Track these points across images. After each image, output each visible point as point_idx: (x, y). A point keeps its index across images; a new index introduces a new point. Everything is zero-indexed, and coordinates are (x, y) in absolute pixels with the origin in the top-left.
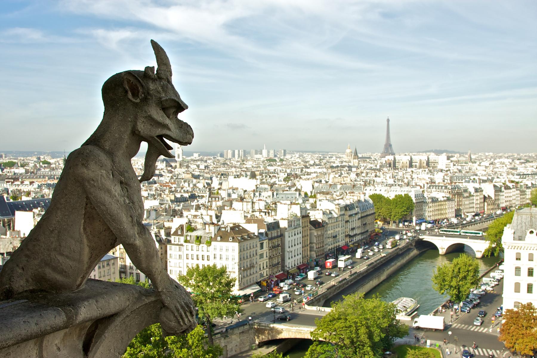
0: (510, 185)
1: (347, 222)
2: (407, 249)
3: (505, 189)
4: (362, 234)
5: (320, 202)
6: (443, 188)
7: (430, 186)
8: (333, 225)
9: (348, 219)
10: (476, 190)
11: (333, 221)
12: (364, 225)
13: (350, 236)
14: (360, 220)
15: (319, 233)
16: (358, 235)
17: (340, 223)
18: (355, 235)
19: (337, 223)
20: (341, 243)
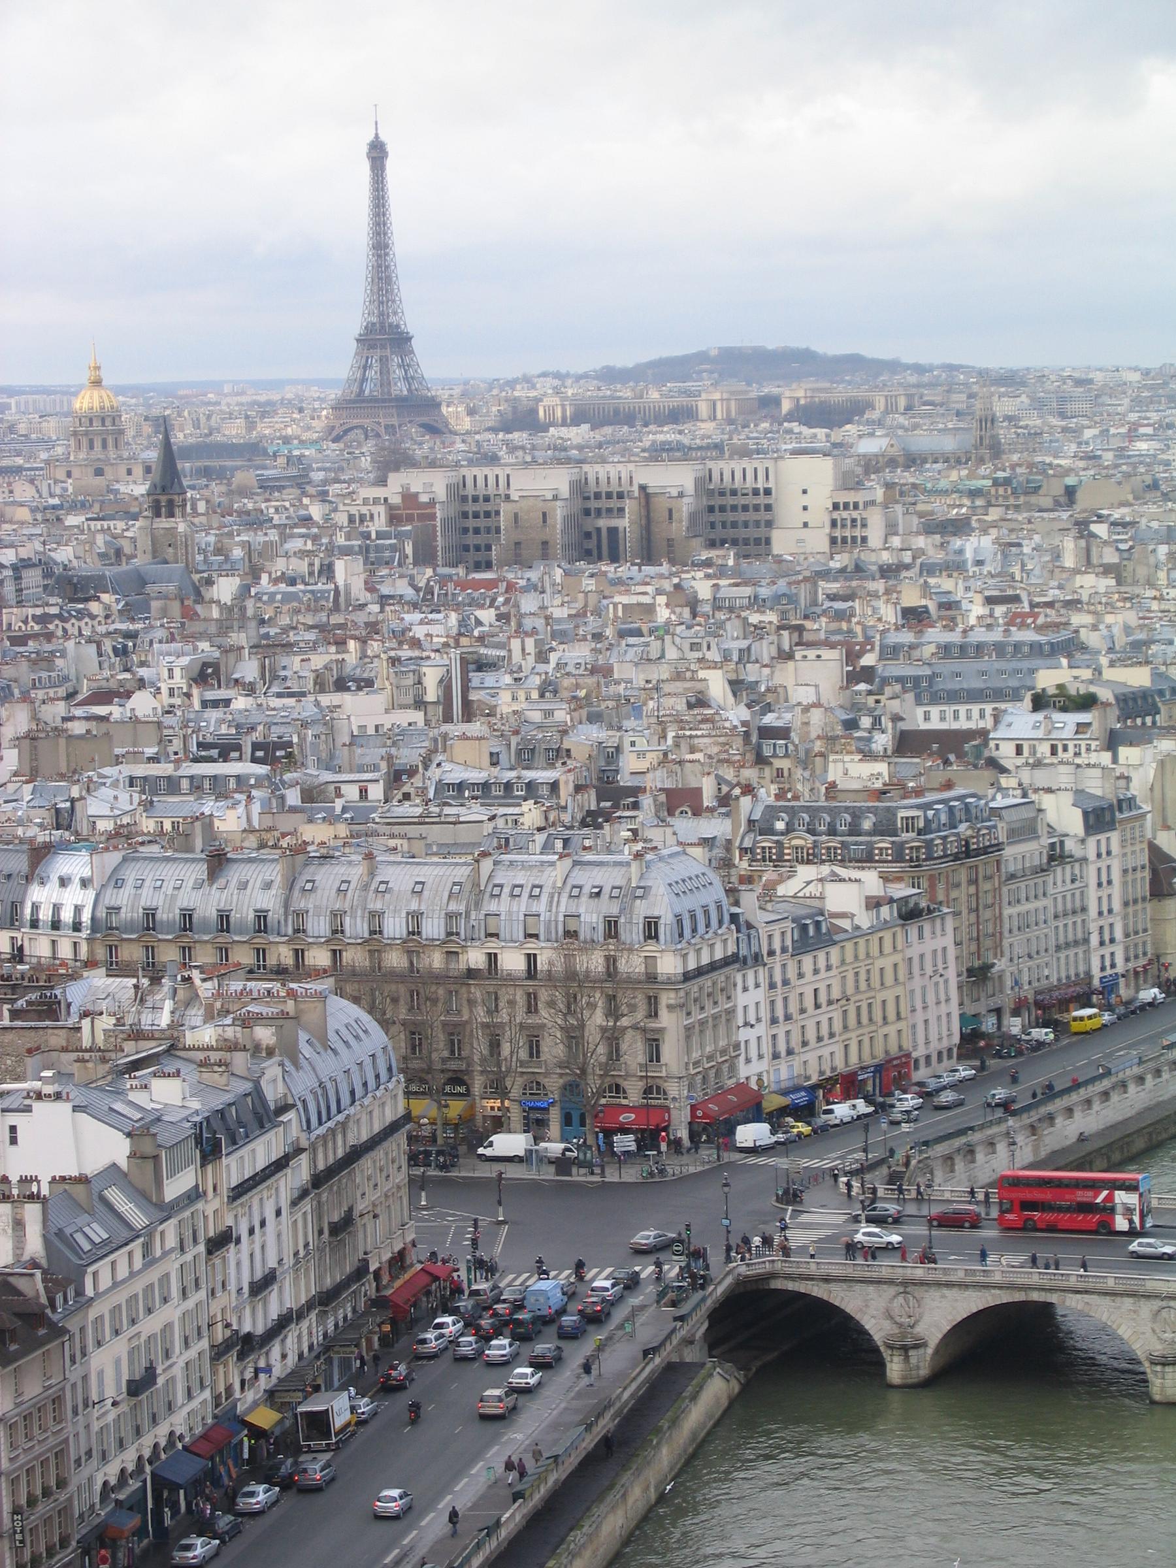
4: (325, 1300)
7: (771, 813)
8: (120, 1297)
10: (1099, 818)
11: (122, 1272)
14: (307, 1206)
15: (33, 1389)
17: (172, 1266)
19: (153, 1275)
20: (186, 1417)
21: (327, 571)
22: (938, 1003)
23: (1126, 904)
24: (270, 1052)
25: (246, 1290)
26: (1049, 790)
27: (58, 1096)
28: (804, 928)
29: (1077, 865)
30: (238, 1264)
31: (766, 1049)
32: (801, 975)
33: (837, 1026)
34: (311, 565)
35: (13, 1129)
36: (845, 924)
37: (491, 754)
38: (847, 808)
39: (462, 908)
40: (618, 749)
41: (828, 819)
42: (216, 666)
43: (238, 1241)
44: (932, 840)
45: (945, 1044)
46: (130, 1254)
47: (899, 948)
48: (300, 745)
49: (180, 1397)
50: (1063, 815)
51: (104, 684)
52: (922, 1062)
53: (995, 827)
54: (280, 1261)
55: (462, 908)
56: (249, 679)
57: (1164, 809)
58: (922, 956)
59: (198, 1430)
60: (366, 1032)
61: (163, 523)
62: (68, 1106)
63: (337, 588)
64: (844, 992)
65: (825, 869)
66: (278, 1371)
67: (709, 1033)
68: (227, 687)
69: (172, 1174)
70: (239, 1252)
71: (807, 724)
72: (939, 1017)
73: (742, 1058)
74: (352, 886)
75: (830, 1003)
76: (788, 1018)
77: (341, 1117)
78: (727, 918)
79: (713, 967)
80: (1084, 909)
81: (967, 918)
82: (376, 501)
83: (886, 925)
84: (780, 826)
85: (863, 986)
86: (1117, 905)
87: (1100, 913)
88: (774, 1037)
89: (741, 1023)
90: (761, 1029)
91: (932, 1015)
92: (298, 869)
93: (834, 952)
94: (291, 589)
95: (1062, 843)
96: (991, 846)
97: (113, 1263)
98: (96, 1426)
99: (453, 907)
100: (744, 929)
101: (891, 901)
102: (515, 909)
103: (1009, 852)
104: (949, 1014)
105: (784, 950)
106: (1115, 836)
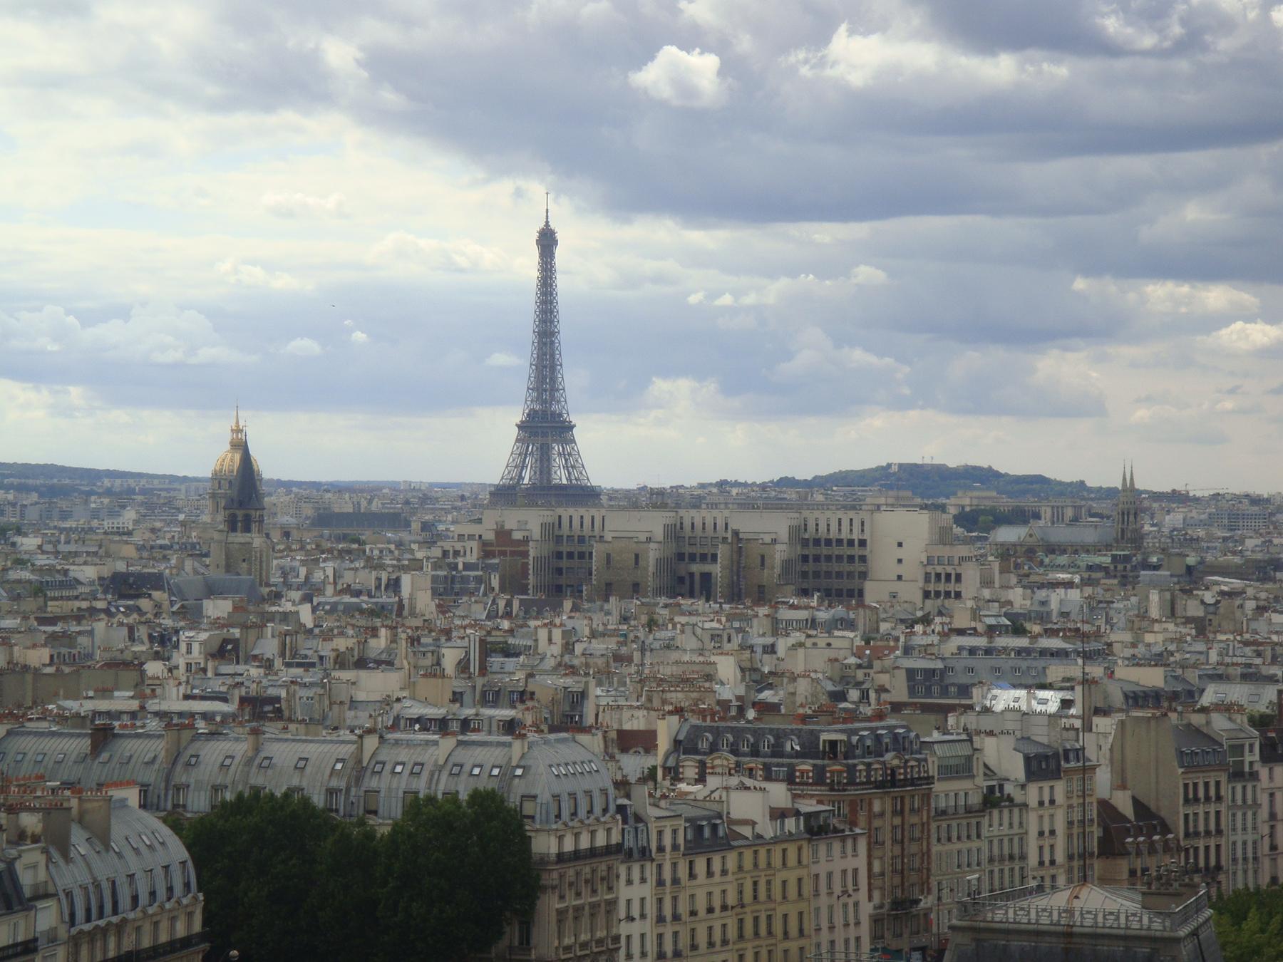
7: (696, 732)
10: (1043, 765)
21: (394, 585)
22: (847, 925)
23: (1070, 857)
24: (35, 839)
26: (991, 734)
29: (1016, 811)
32: (692, 876)
33: (732, 933)
34: (379, 579)
36: (746, 831)
37: (454, 693)
38: (771, 730)
39: (343, 785)
40: (583, 695)
41: (752, 740)
42: (236, 642)
44: (855, 765)
47: (805, 862)
48: (288, 700)
50: (1004, 759)
51: (118, 655)
53: (926, 760)
55: (343, 785)
56: (269, 655)
57: (1123, 770)
58: (830, 875)
60: (162, 844)
61: (239, 538)
63: (401, 600)
64: (741, 899)
65: (734, 781)
67: (585, 921)
68: (246, 663)
71: (794, 694)
72: (847, 941)
73: (622, 952)
74: (236, 761)
75: (724, 908)
76: (676, 918)
77: (115, 919)
78: (612, 808)
79: (593, 853)
80: (1023, 857)
81: (889, 849)
82: (471, 537)
83: (790, 838)
84: (704, 746)
85: (762, 895)
86: (1060, 857)
87: (1041, 863)
88: (660, 936)
89: (622, 915)
90: (647, 927)
92: (184, 743)
93: (732, 860)
94: (354, 600)
95: (1001, 787)
96: (920, 778)
99: (334, 783)
100: (631, 821)
101: (797, 813)
102: (394, 786)
103: (938, 787)
104: (858, 939)
105: (675, 847)
106: (1060, 787)
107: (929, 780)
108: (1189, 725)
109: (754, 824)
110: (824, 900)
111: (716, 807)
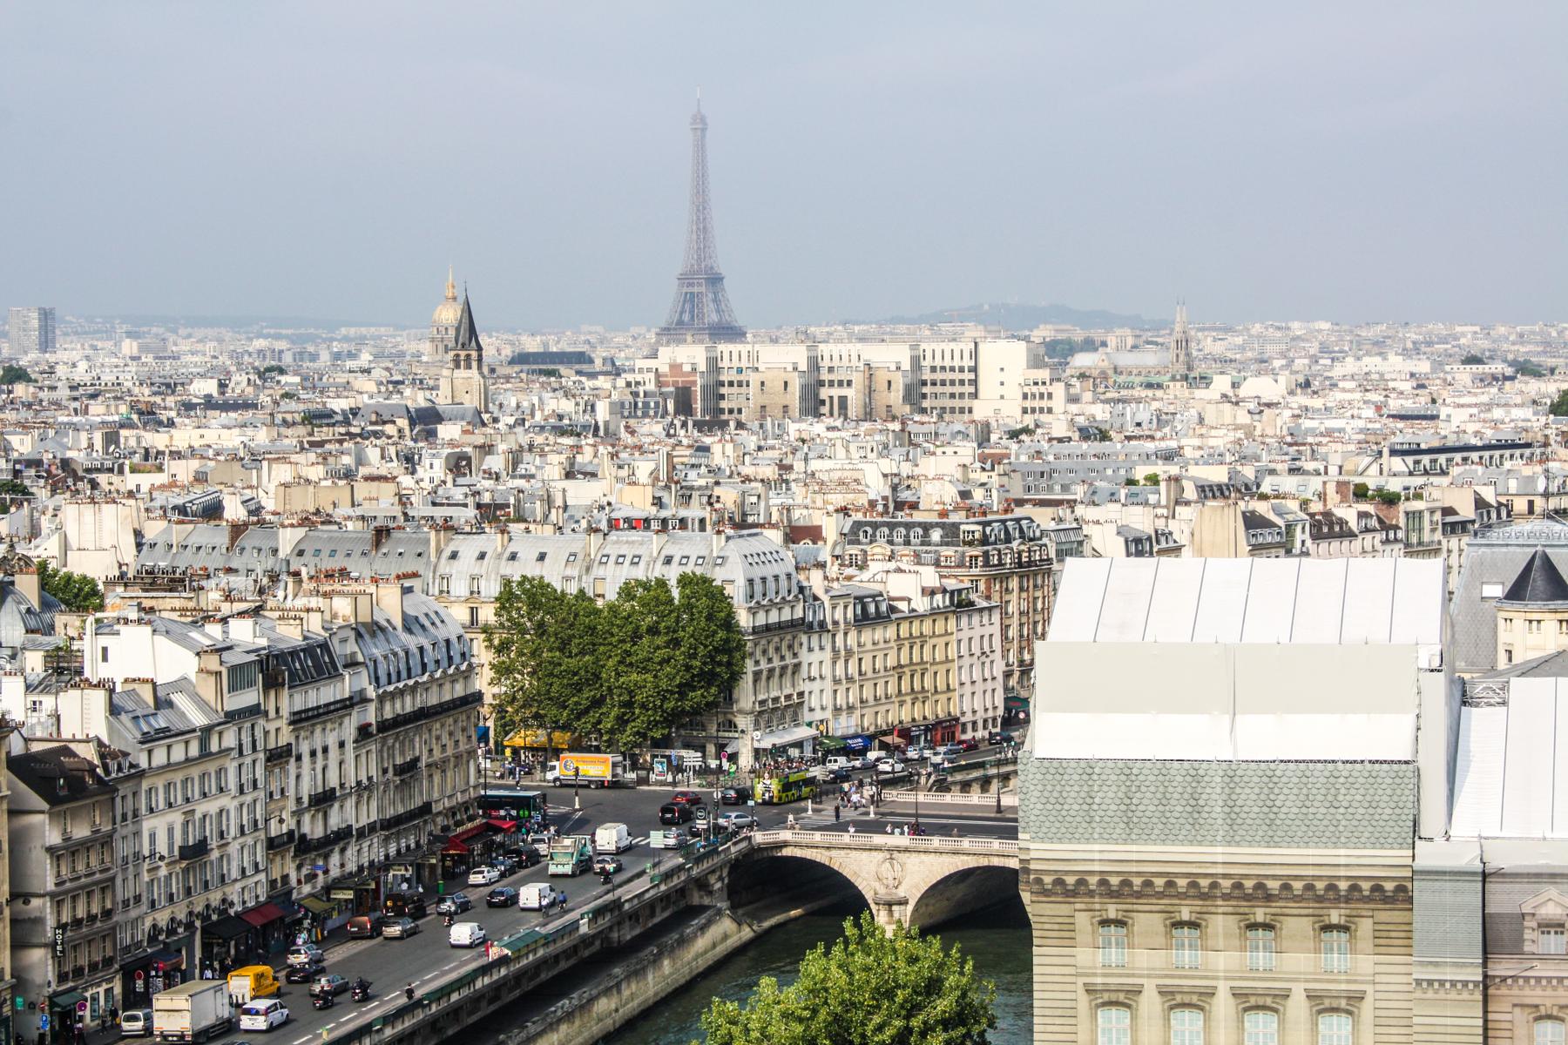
0: (1348, 513)
1: (278, 757)
2: (675, 912)
3: (1317, 536)
4: (390, 826)
5: (104, 641)
6: (936, 535)
8: (178, 777)
9: (286, 737)
11: (178, 754)
12: (401, 770)
13: (303, 846)
15: (81, 831)
16: (361, 834)
18: (342, 836)
19: (212, 767)
25: (306, 800)
26: (1098, 522)
27: (139, 621)
28: (864, 609)
30: (298, 777)
31: (827, 699)
35: (105, 650)
36: (903, 606)
43: (299, 758)
45: (990, 714)
46: (187, 743)
49: (235, 874)
52: (969, 726)
54: (342, 785)
59: (251, 904)
62: (148, 629)
66: (335, 872)
69: (233, 688)
70: (299, 767)
76: (850, 679)
79: (781, 627)
82: (649, 370)
90: (828, 685)
91: (979, 687)
93: (891, 632)
97: (169, 747)
98: (146, 877)
101: (944, 591)
107: (1049, 560)
108: (1253, 512)
109: (909, 600)
110: (966, 661)
111: (877, 587)
